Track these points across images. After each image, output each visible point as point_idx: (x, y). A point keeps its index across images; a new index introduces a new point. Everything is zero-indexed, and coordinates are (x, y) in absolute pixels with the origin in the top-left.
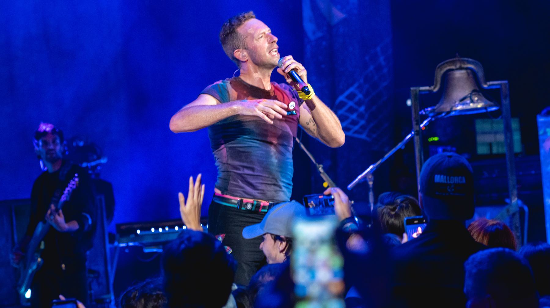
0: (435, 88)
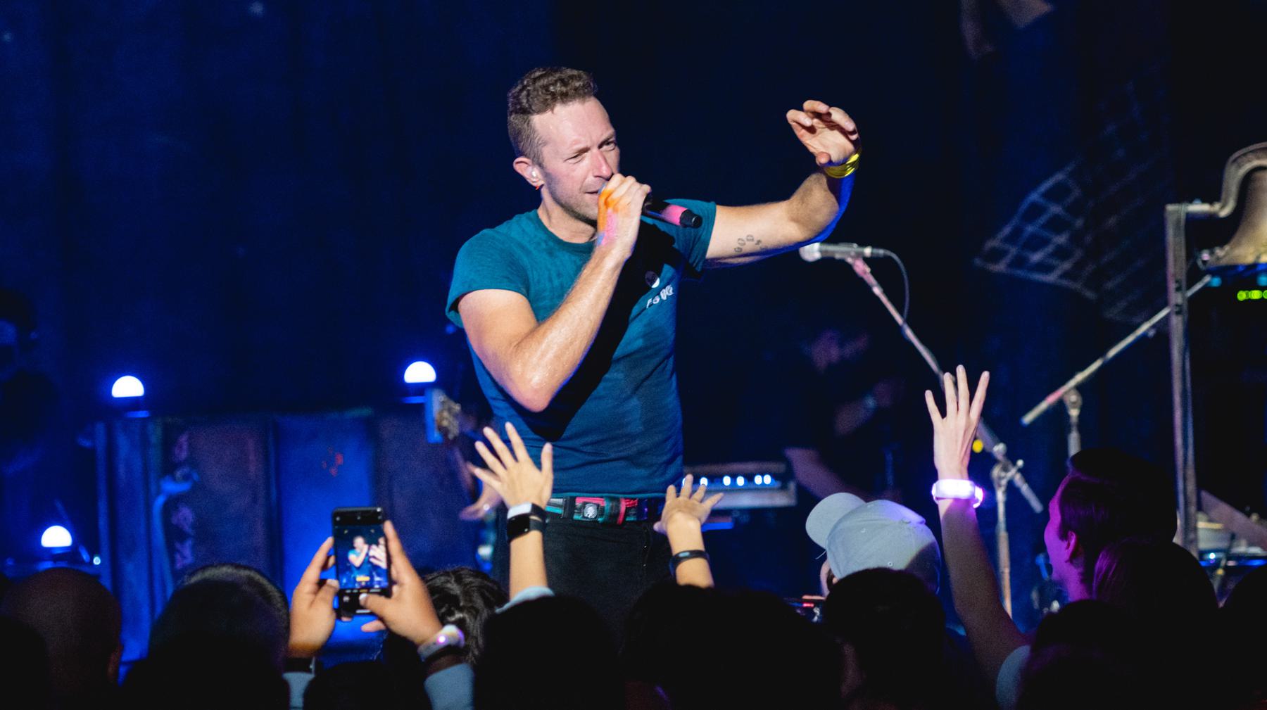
0: (1223, 207)
